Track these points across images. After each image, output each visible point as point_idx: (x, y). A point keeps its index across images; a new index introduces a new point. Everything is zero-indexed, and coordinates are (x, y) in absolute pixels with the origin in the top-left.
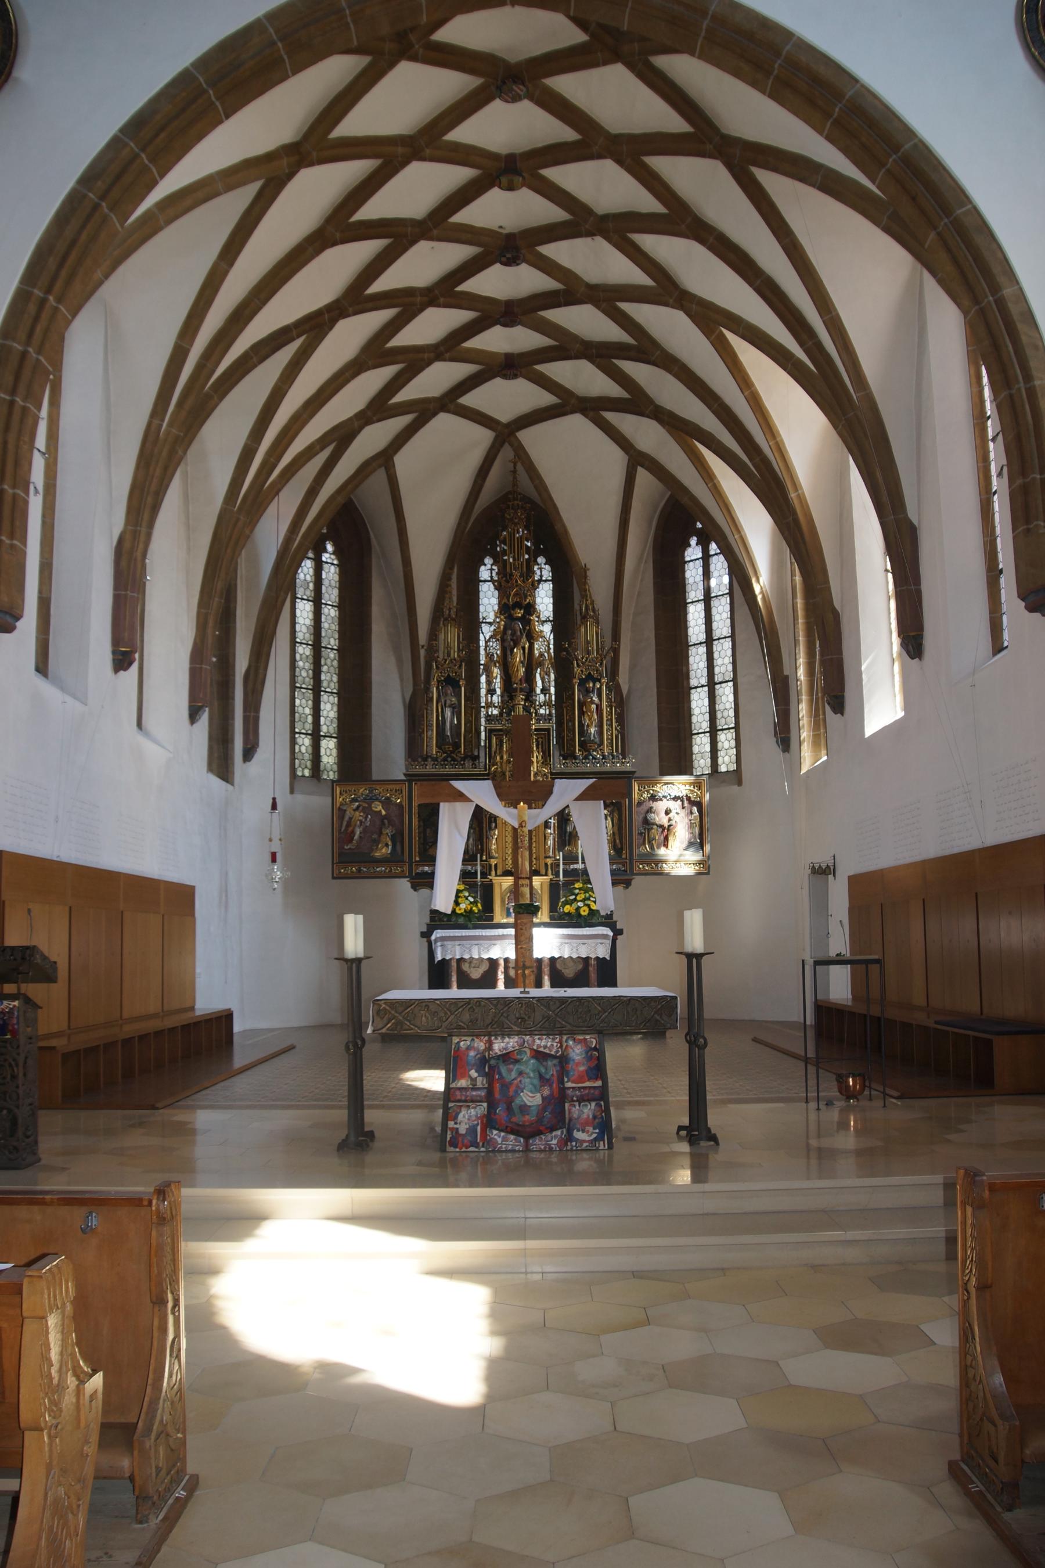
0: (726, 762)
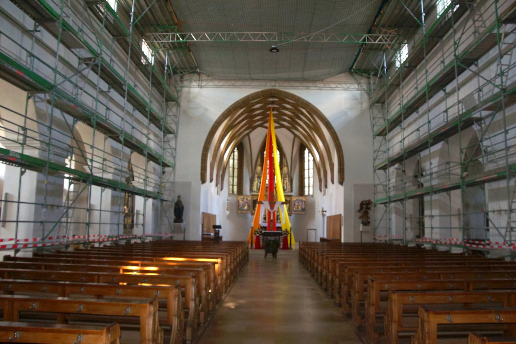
0: (311, 193)
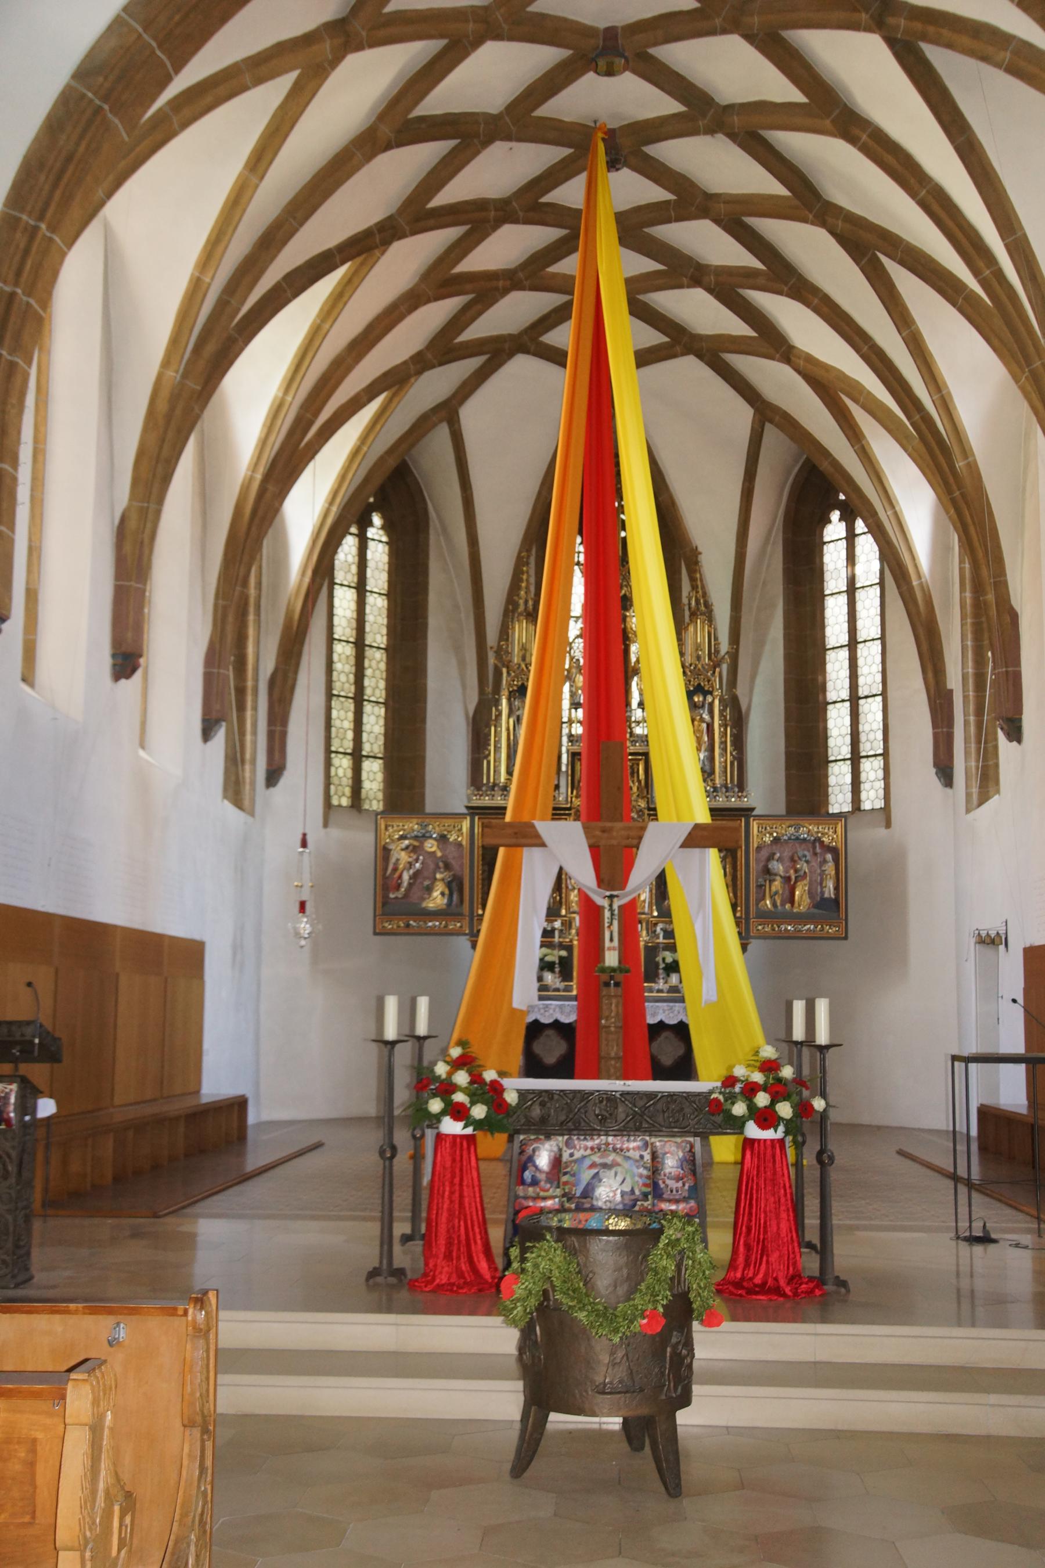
0: (872, 797)
